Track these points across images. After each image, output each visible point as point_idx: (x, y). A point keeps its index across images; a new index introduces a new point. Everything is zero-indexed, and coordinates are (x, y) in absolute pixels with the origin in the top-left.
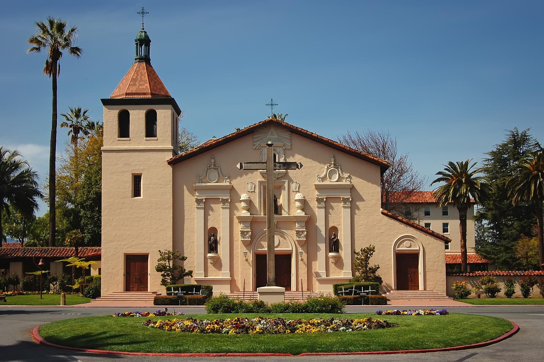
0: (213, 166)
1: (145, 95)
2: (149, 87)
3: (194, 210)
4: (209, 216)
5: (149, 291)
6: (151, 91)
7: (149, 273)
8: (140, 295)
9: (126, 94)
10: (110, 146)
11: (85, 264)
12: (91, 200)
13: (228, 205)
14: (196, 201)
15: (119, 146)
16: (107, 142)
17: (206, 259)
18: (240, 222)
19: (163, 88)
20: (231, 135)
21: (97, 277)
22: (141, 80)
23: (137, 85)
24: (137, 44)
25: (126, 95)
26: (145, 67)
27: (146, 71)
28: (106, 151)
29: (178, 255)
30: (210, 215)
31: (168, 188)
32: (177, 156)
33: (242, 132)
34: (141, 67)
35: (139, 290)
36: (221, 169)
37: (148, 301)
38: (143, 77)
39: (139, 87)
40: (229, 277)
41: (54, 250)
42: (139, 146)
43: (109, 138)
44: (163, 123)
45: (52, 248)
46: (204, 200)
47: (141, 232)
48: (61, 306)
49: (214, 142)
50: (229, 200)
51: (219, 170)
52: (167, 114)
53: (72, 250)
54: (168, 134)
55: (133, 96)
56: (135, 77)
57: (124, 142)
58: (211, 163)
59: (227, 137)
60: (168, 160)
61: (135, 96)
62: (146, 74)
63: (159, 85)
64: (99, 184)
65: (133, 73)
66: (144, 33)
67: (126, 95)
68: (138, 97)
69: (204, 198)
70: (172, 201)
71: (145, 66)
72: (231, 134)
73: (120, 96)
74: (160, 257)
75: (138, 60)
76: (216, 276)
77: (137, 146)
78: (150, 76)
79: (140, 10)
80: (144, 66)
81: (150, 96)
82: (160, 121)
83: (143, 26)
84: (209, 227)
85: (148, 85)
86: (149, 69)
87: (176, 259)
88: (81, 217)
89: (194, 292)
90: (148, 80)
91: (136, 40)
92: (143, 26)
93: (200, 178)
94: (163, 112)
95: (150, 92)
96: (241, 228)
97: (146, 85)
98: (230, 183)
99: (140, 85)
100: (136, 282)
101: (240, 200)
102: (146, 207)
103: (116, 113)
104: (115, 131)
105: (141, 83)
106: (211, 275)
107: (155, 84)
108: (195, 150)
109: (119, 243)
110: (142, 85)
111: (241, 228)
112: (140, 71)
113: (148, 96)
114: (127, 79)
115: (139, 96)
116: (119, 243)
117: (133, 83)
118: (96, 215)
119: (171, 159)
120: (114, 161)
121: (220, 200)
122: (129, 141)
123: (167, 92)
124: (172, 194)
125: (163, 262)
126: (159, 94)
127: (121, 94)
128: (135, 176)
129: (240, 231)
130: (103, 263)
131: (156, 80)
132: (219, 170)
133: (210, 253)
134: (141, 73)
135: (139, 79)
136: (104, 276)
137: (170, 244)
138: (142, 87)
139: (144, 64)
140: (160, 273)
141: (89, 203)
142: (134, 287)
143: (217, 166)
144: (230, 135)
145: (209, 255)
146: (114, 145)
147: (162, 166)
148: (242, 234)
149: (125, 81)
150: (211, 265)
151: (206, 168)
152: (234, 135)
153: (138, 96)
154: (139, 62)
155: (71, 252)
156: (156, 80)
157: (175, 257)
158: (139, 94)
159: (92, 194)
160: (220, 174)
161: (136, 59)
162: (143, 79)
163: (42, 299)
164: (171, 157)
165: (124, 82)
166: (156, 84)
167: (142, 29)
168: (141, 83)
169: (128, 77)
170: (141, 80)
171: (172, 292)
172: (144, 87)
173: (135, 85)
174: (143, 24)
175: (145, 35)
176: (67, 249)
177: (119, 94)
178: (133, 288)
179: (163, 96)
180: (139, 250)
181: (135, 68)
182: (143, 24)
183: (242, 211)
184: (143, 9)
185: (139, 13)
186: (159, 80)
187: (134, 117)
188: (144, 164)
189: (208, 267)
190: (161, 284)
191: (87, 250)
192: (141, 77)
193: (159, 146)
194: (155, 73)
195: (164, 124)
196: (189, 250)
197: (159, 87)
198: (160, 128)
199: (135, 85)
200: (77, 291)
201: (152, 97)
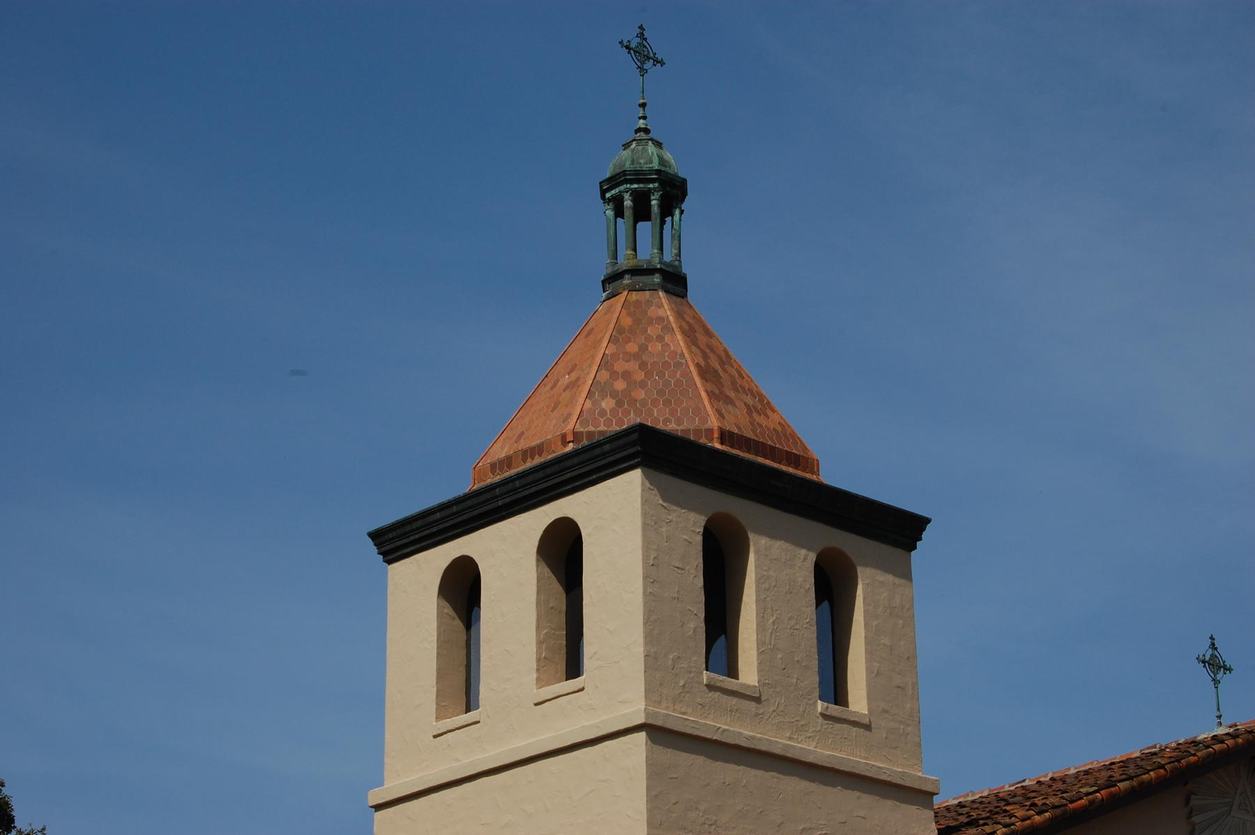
9: (725, 436)
10: (674, 710)
43: (670, 662)
57: (734, 701)
75: (657, 279)
77: (790, 738)
82: (875, 623)
94: (882, 583)
103: (694, 523)
104: (692, 625)
108: (1037, 818)
122: (753, 704)
146: (690, 710)
158: (771, 452)
187: (771, 573)
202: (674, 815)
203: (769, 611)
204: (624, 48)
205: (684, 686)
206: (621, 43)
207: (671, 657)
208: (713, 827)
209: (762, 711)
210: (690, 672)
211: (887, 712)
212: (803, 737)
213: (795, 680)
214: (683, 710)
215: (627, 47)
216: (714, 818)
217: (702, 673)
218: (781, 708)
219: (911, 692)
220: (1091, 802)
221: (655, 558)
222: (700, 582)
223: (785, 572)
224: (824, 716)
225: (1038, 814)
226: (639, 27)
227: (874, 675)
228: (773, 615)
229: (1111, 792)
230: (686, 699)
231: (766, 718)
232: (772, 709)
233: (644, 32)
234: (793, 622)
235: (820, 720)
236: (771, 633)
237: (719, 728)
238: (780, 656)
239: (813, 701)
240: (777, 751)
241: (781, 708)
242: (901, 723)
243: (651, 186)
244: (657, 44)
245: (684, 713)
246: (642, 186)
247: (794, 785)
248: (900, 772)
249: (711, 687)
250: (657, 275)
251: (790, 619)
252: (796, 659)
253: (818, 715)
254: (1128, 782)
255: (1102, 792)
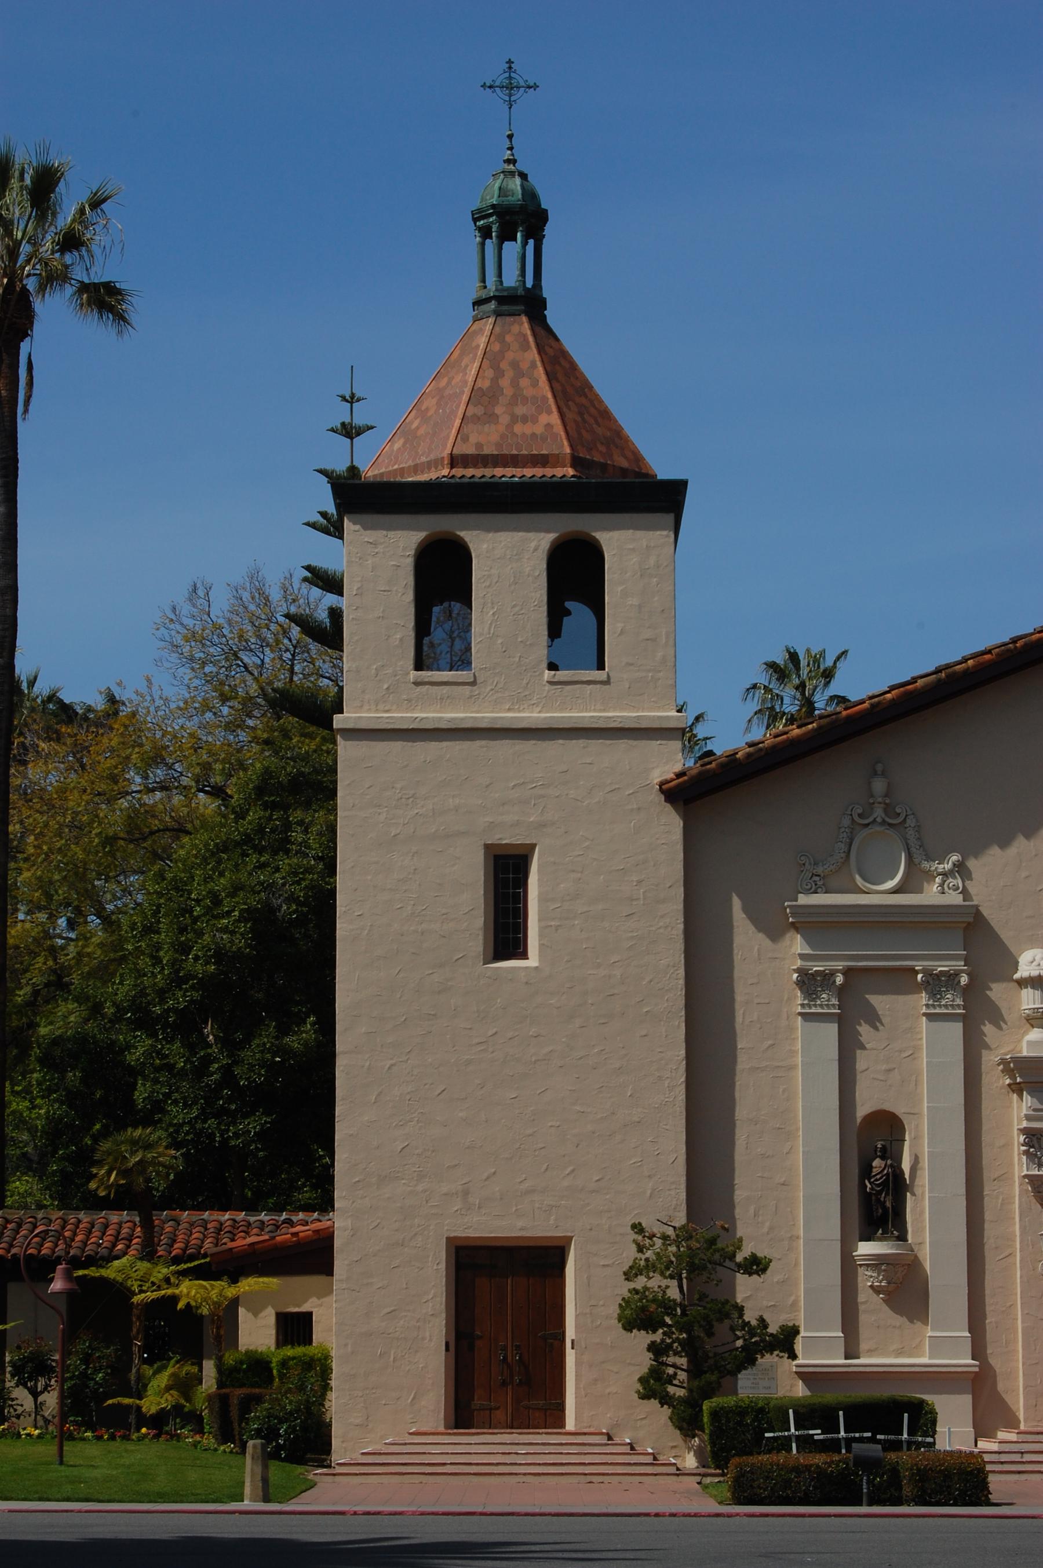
0: (879, 813)
1: (544, 466)
2: (559, 429)
3: (792, 1029)
4: (858, 1052)
5: (570, 1425)
6: (571, 446)
7: (570, 1333)
8: (552, 1449)
9: (454, 461)
10: (377, 711)
11: (218, 1290)
12: (193, 987)
13: (952, 1001)
14: (801, 984)
15: (421, 711)
16: (363, 692)
17: (849, 1266)
18: (1017, 1089)
19: (617, 438)
20: (970, 662)
21: (294, 1358)
22: (518, 398)
23: (500, 420)
24: (485, 233)
25: (452, 468)
26: (531, 339)
27: (537, 358)
28: (355, 733)
29: (731, 1248)
30: (863, 1047)
31: (662, 917)
32: (710, 763)
33: (1026, 644)
34: (508, 338)
35: (519, 1422)
36: (918, 828)
37: (600, 1479)
38: (524, 382)
39: (510, 427)
40: (965, 1361)
41: (19, 1225)
42: (519, 711)
43: (373, 671)
44: (635, 601)
45: (10, 1217)
46: (839, 979)
47: (529, 1131)
48: (247, 1504)
49: (889, 696)
50: (964, 979)
51: (911, 834)
52: (652, 561)
53: (106, 1226)
54: (660, 654)
55: (488, 472)
56: (485, 384)
57: (445, 689)
58: (872, 796)
59: (955, 673)
60: (667, 782)
61: (499, 472)
62: (541, 369)
63: (600, 420)
64: (228, 914)
65: (476, 365)
66: (518, 180)
67: (452, 468)
68: (513, 476)
69: (840, 965)
70: (682, 982)
71: (529, 332)
72: (974, 656)
73: (416, 469)
74: (630, 1254)
75: (493, 305)
76: (899, 1353)
77: (509, 710)
78: (558, 381)
79: (496, 73)
80: (525, 336)
81: (571, 472)
82: (620, 589)
83: (511, 149)
84: (862, 1110)
85: (555, 419)
86: (547, 348)
87: (718, 1268)
88: (134, 1072)
89: (905, 1436)
90: (550, 395)
91: (480, 210)
92: (511, 149)
93: (819, 870)
94: (633, 549)
95: (568, 450)
96: (1028, 1118)
97: (544, 419)
98: (965, 892)
99: (514, 419)
100: (504, 1384)
101: (1017, 976)
102: (558, 1008)
103: (404, 549)
105: (520, 410)
106: (876, 1349)
107: (581, 414)
109: (420, 1188)
110: (525, 419)
111: (1028, 1118)
112: (510, 355)
113: (559, 472)
114: (448, 392)
115: (518, 472)
116: (420, 1188)
117: (479, 411)
118: (216, 1060)
119: (679, 775)
120: (398, 786)
121: (920, 976)
123: (637, 458)
124: (680, 946)
125: (656, 1282)
126: (606, 464)
127: (424, 459)
128: (497, 858)
129: (1025, 1131)
130: (344, 1286)
131: (583, 400)
132: (911, 834)
133: (867, 1238)
134: (515, 365)
135: (508, 392)
136: (349, 1349)
137: (673, 1193)
138: (528, 429)
139: (524, 325)
140: (642, 1339)
141: (180, 999)
142: (498, 1408)
143: (898, 810)
144: (965, 660)
145: (865, 1248)
146: (394, 707)
147: (632, 810)
148: (1033, 1147)
149: (434, 401)
150: (878, 1299)
151: (846, 822)
152: (989, 661)
153: (509, 471)
154: (498, 314)
155: (104, 1234)
156: (583, 400)
157: (717, 1256)
158: (514, 461)
159: (196, 958)
160: (913, 850)
161: (478, 303)
162: (529, 392)
163: (63, 1468)
164: (678, 768)
165: (427, 409)
166: (586, 416)
167: (508, 161)
168: (520, 410)
169: (449, 383)
170: (515, 399)
171: (789, 1438)
172: (539, 429)
173: (491, 418)
174: (510, 137)
175: (522, 186)
176: (79, 1221)
177: (411, 463)
178: (491, 1409)
179: (624, 472)
180: (520, 1224)
181: (482, 341)
182: (510, 137)
183: (1026, 1033)
184: (510, 68)
185: (490, 87)
186: (596, 403)
187: (493, 571)
188: (542, 796)
189: (861, 1308)
190: (638, 1392)
191: (179, 1225)
192: (515, 383)
193: (615, 709)
194: (573, 366)
195: (640, 606)
196: (767, 1224)
197: (599, 431)
198: (620, 625)
199: (491, 418)
200: (158, 1422)
201: (580, 477)
202: (368, 797)
203: (490, 605)
204: (488, 89)
205: (388, 688)
206: (484, 86)
207: (375, 667)
208: (411, 800)
209: (477, 692)
210: (395, 676)
211: (632, 664)
212: (526, 706)
213: (517, 659)
214: (386, 708)
215: (490, 87)
216: (412, 792)
217: (408, 673)
218: (500, 685)
219: (664, 641)
220: (872, 706)
221: (359, 588)
222: (410, 596)
223: (510, 567)
224: (550, 683)
225: (799, 727)
226: (507, 63)
227: (617, 635)
228: (493, 608)
229: (907, 690)
230: (391, 698)
231: (482, 697)
232: (489, 688)
233: (513, 65)
234: (517, 609)
235: (547, 687)
236: (491, 624)
237: (417, 718)
238: (499, 641)
239: (537, 673)
240: (484, 725)
241: (500, 685)
242: (649, 671)
243: (491, 220)
244: (524, 73)
245: (387, 711)
246: (485, 221)
247: (504, 748)
248: (635, 717)
249: (417, 684)
250: (493, 302)
251: (514, 606)
252: (519, 640)
253: (545, 683)
254: (934, 676)
255: (893, 692)
